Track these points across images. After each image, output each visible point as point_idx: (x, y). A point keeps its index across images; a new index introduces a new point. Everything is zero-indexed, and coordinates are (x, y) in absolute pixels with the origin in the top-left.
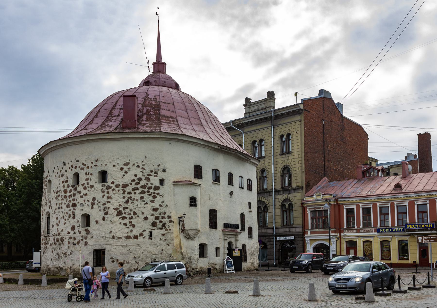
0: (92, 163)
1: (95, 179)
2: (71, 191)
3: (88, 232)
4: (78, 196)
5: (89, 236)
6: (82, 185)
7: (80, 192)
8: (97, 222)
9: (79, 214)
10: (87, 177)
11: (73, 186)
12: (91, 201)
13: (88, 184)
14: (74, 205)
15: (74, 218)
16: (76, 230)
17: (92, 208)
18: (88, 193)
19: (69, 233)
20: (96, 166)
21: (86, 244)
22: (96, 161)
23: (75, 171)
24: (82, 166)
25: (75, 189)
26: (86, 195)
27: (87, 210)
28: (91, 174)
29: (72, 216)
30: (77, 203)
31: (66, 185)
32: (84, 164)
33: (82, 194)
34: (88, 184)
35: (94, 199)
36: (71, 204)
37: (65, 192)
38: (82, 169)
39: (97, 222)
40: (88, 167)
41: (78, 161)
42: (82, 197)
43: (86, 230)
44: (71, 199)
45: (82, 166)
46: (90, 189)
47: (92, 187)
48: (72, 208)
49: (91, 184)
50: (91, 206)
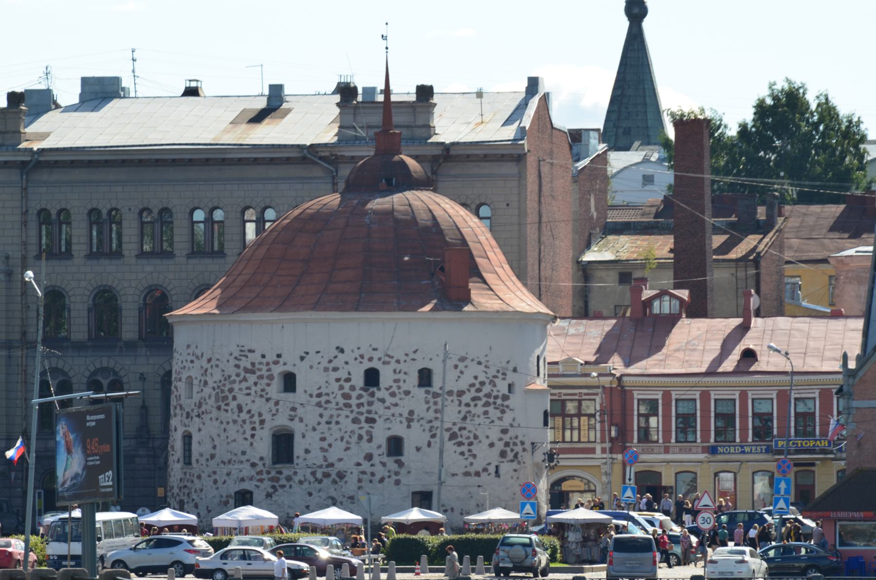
0: (407, 355)
1: (413, 379)
2: (360, 397)
3: (400, 464)
4: (377, 407)
5: (403, 471)
6: (387, 389)
7: (383, 401)
8: (418, 449)
9: (381, 435)
10: (397, 376)
11: (361, 389)
12: (406, 415)
13: (399, 388)
14: (371, 421)
15: (370, 440)
16: (376, 460)
17: (409, 427)
18: (399, 402)
19: (359, 464)
20: (414, 360)
21: (397, 482)
22: (415, 352)
23: (367, 365)
24: (387, 359)
25: (372, 395)
26: (396, 405)
27: (398, 429)
28: (405, 373)
29: (365, 437)
30: (376, 417)
31: (347, 386)
32: (389, 356)
33: (387, 404)
34: (399, 388)
35: (411, 413)
36: (362, 418)
37: (346, 396)
38: (388, 363)
39: (418, 449)
40: (398, 362)
41: (375, 349)
42: (388, 408)
43: (396, 461)
44: (363, 409)
45: (387, 359)
46: (403, 396)
47: (407, 393)
48: (366, 426)
49: (405, 387)
50: (405, 424)
